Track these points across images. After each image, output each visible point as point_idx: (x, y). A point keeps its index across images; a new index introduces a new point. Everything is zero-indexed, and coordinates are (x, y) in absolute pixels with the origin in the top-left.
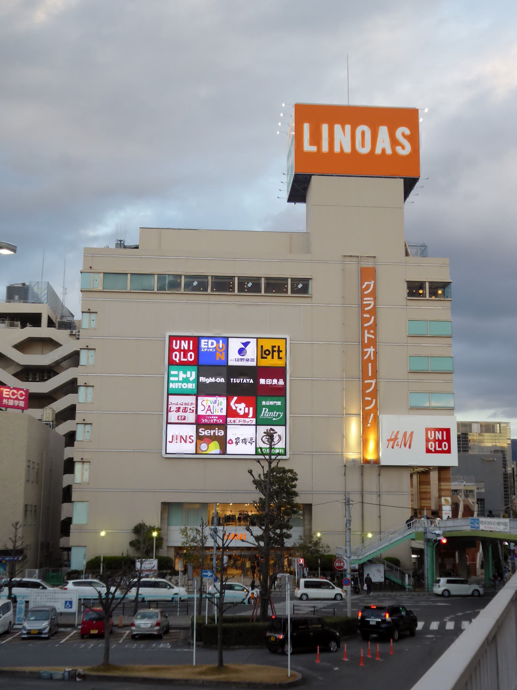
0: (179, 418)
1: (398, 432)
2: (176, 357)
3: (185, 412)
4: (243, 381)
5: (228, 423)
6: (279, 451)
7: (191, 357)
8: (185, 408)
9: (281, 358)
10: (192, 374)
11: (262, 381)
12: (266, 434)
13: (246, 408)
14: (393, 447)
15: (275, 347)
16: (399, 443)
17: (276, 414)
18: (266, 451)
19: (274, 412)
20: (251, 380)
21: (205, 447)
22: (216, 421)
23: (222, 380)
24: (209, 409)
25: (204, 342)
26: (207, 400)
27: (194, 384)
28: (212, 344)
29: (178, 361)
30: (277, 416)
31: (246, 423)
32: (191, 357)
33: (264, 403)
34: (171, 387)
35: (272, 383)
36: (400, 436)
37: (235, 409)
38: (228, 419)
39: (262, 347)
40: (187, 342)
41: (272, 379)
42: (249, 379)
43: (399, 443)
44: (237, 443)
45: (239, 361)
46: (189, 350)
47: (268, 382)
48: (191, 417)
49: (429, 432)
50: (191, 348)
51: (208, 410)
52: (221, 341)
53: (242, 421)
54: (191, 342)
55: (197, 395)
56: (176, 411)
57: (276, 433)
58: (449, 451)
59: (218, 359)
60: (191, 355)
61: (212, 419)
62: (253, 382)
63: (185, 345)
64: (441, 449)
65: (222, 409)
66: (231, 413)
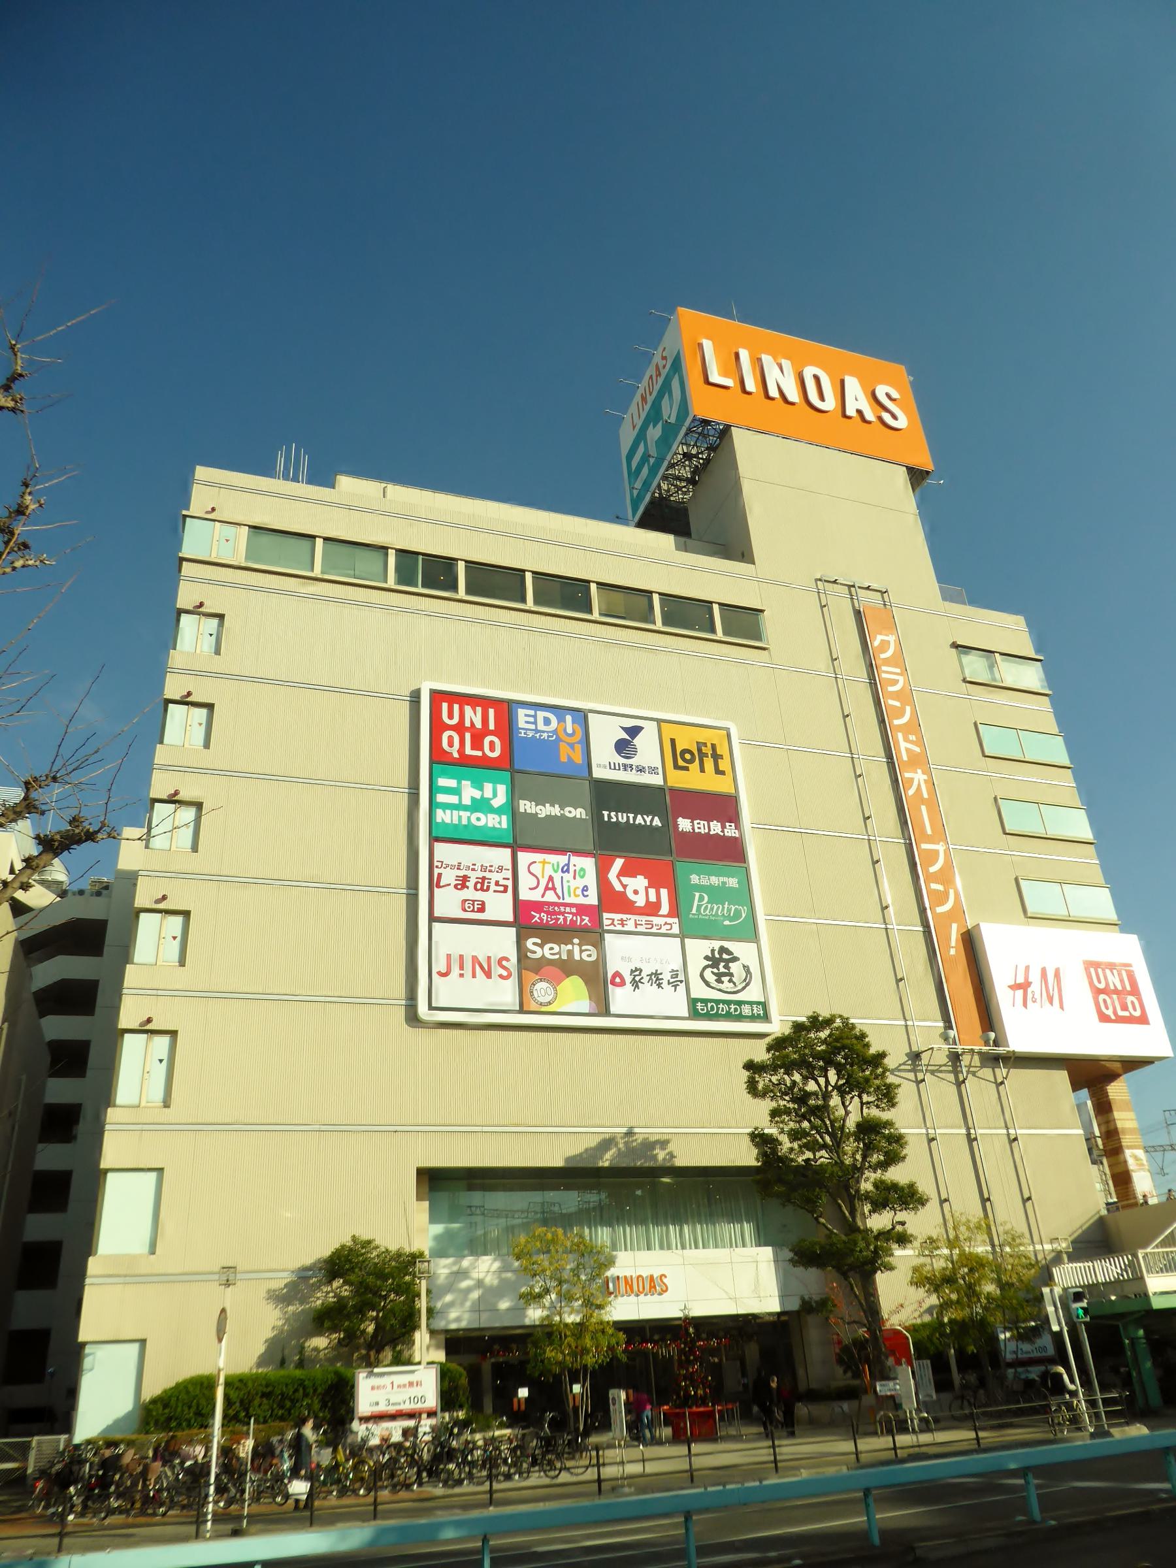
0: (467, 905)
1: (1027, 968)
2: (451, 744)
3: (482, 889)
4: (635, 819)
5: (605, 928)
6: (752, 1010)
7: (493, 747)
8: (484, 878)
9: (723, 773)
10: (496, 793)
11: (684, 824)
12: (710, 963)
13: (649, 889)
14: (1025, 1005)
15: (705, 745)
16: (1037, 996)
17: (729, 910)
18: (718, 1009)
19: (723, 905)
20: (656, 818)
21: (546, 993)
22: (571, 920)
23: (579, 813)
24: (550, 885)
25: (526, 715)
26: (544, 862)
27: (504, 818)
28: (547, 721)
29: (456, 755)
30: (732, 915)
31: (654, 930)
32: (492, 749)
33: (695, 879)
34: (439, 820)
35: (709, 830)
36: (1035, 977)
37: (621, 889)
38: (606, 915)
39: (673, 741)
40: (479, 709)
41: (709, 820)
42: (650, 817)
43: (1037, 996)
44: (636, 984)
45: (619, 770)
46: (485, 731)
47: (699, 828)
48: (500, 907)
49: (1092, 970)
50: (492, 727)
51: (547, 889)
52: (569, 718)
53: (643, 923)
54: (491, 712)
55: (515, 847)
56: (456, 886)
57: (735, 959)
58: (1143, 1020)
59: (564, 759)
60: (492, 744)
61: (561, 913)
62: (660, 825)
63: (473, 716)
64: (1126, 1014)
65: (585, 889)
66: (613, 900)
